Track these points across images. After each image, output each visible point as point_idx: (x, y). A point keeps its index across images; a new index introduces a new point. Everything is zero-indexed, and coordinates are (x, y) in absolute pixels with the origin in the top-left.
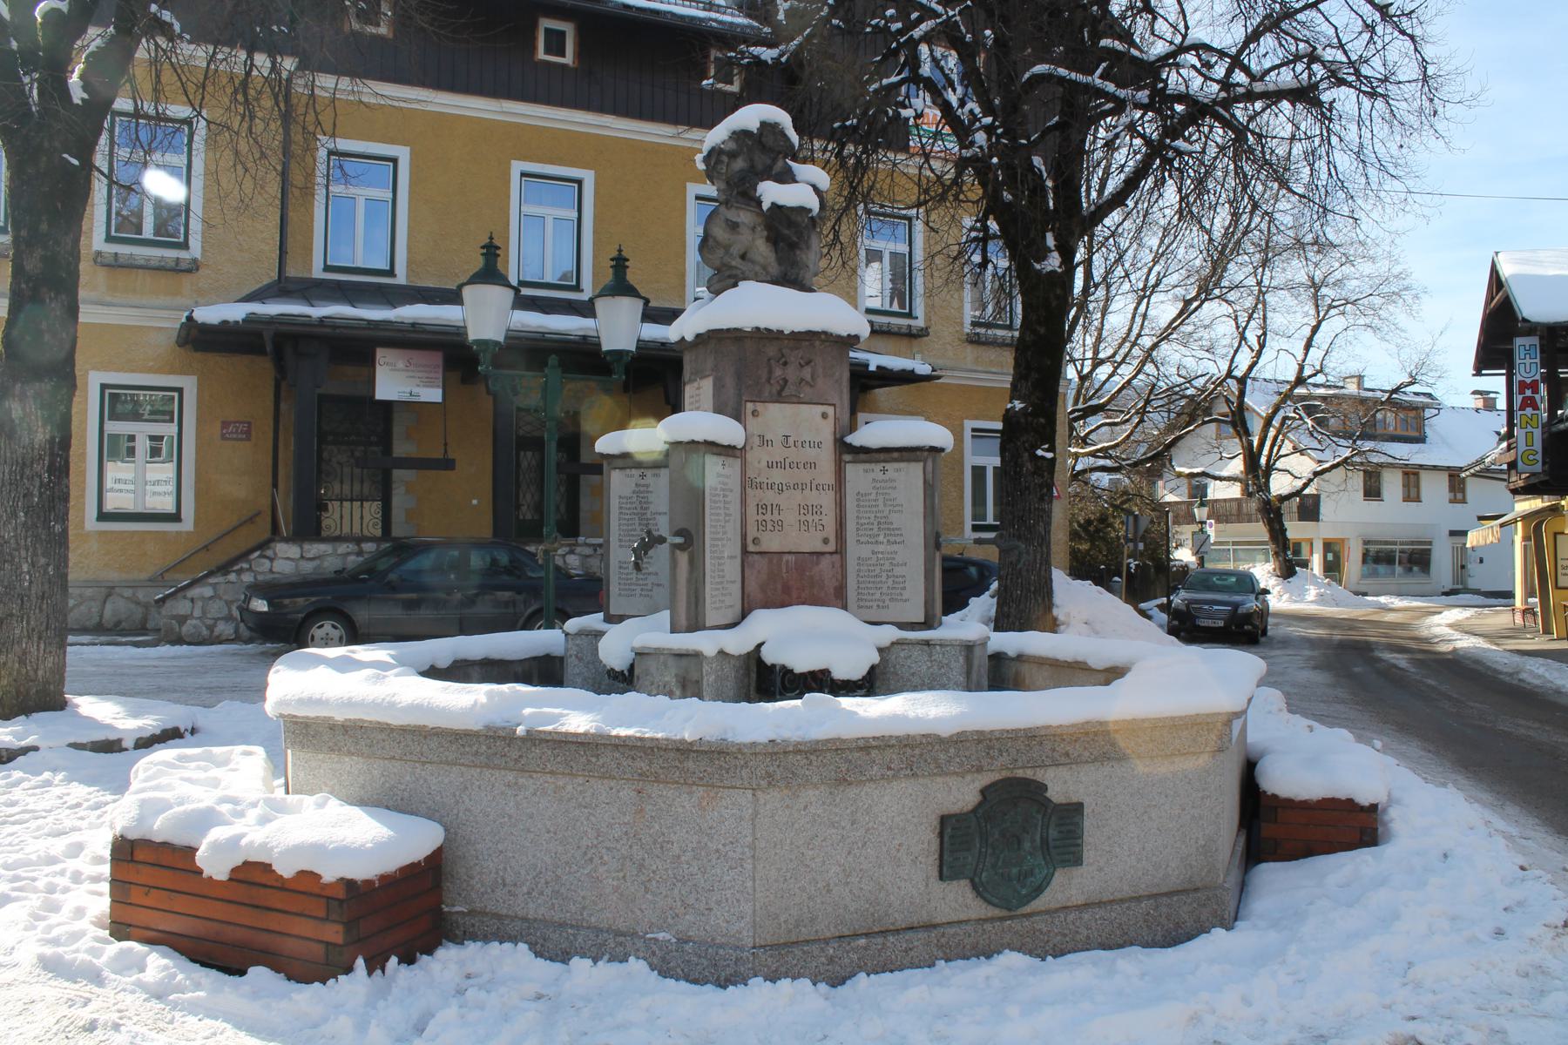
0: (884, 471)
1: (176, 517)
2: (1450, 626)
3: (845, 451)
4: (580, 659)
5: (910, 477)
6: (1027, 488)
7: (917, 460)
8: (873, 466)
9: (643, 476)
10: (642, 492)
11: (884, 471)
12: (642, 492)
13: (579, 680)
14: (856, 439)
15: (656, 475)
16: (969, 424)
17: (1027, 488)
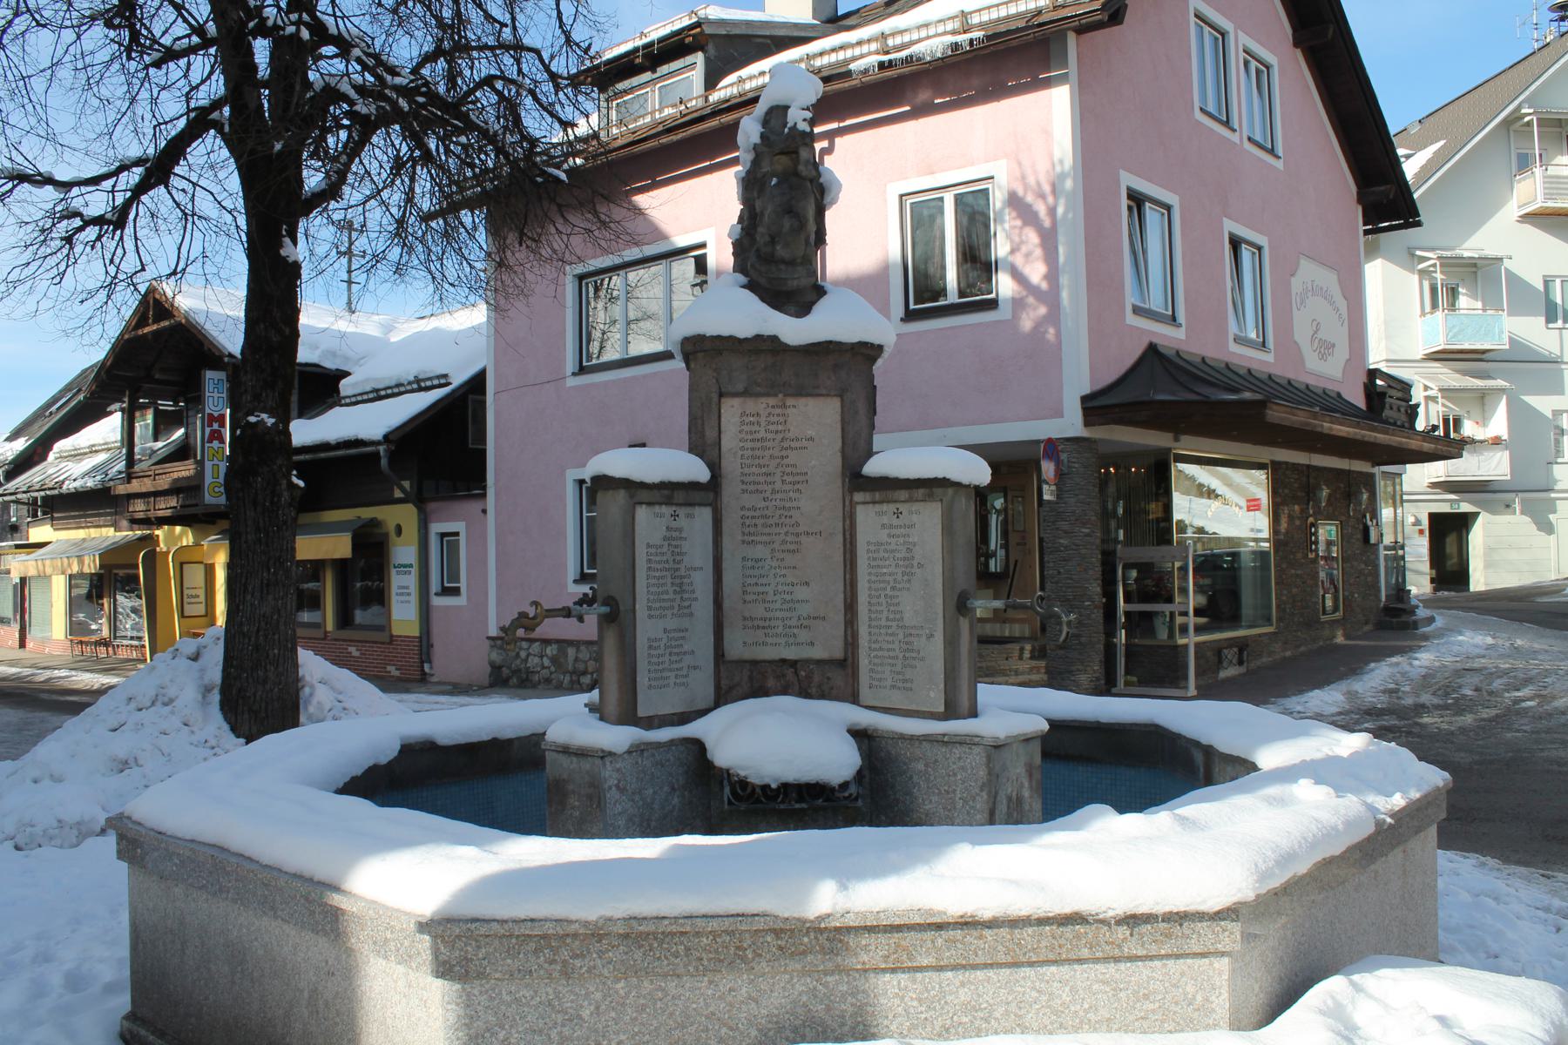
0: (898, 514)
1: (1324, 613)
2: (1241, 767)
3: (856, 481)
4: (622, 790)
5: (926, 521)
6: (285, 523)
7: (929, 497)
8: (885, 507)
9: (675, 516)
10: (674, 538)
11: (898, 514)
12: (674, 538)
13: (621, 822)
14: (873, 467)
15: (689, 516)
16: (381, 448)
17: (285, 523)
